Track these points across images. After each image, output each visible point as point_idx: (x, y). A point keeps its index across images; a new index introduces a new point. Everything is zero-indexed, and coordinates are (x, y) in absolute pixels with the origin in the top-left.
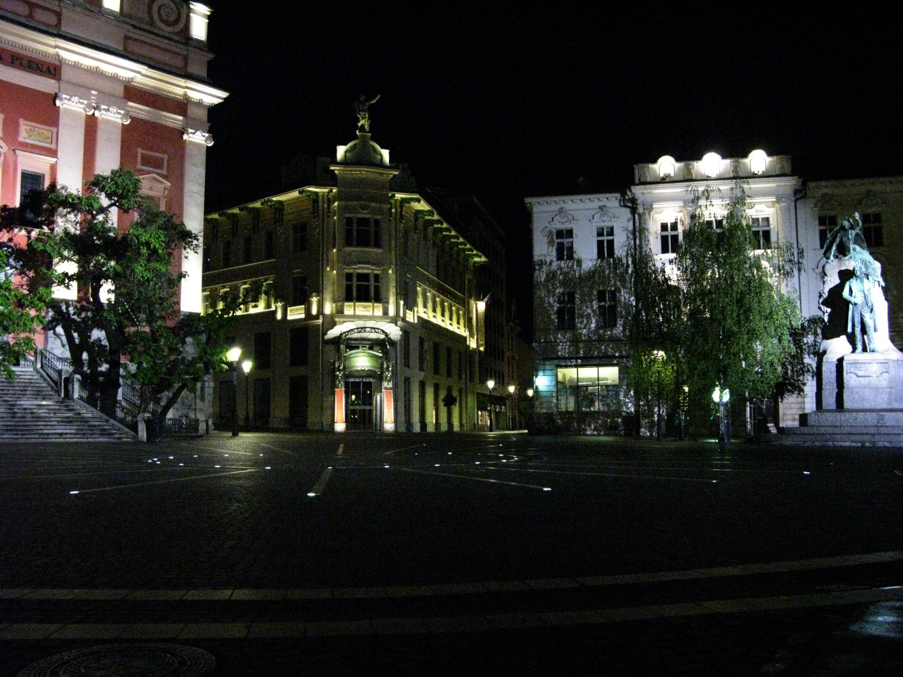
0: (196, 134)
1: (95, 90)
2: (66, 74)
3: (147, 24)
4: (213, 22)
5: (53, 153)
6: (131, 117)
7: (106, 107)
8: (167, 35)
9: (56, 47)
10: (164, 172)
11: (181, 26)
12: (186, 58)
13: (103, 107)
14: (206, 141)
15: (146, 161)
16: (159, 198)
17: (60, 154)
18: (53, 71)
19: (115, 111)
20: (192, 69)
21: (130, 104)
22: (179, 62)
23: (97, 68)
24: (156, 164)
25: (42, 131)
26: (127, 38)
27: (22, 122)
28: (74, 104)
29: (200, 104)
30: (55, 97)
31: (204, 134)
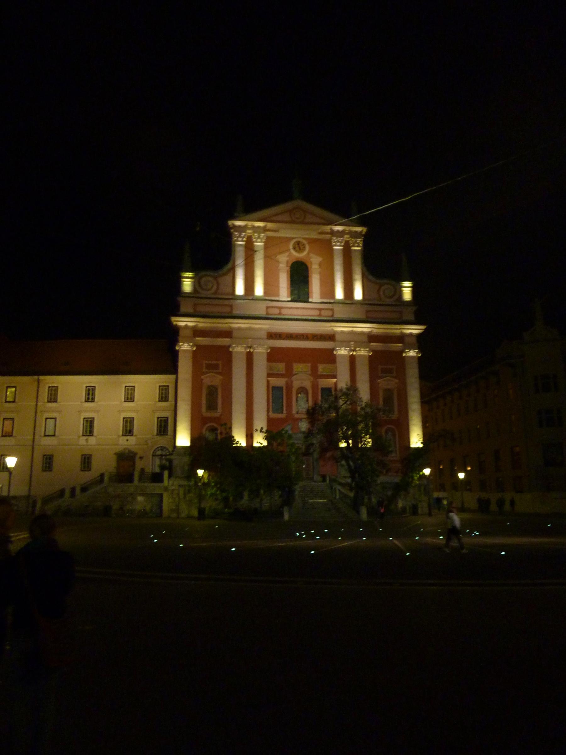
2: (338, 337)
4: (415, 291)
5: (334, 377)
6: (373, 351)
9: (331, 327)
13: (357, 349)
17: (338, 377)
20: (405, 318)
21: (372, 344)
26: (367, 312)
28: (343, 351)
29: (411, 334)
30: (333, 349)
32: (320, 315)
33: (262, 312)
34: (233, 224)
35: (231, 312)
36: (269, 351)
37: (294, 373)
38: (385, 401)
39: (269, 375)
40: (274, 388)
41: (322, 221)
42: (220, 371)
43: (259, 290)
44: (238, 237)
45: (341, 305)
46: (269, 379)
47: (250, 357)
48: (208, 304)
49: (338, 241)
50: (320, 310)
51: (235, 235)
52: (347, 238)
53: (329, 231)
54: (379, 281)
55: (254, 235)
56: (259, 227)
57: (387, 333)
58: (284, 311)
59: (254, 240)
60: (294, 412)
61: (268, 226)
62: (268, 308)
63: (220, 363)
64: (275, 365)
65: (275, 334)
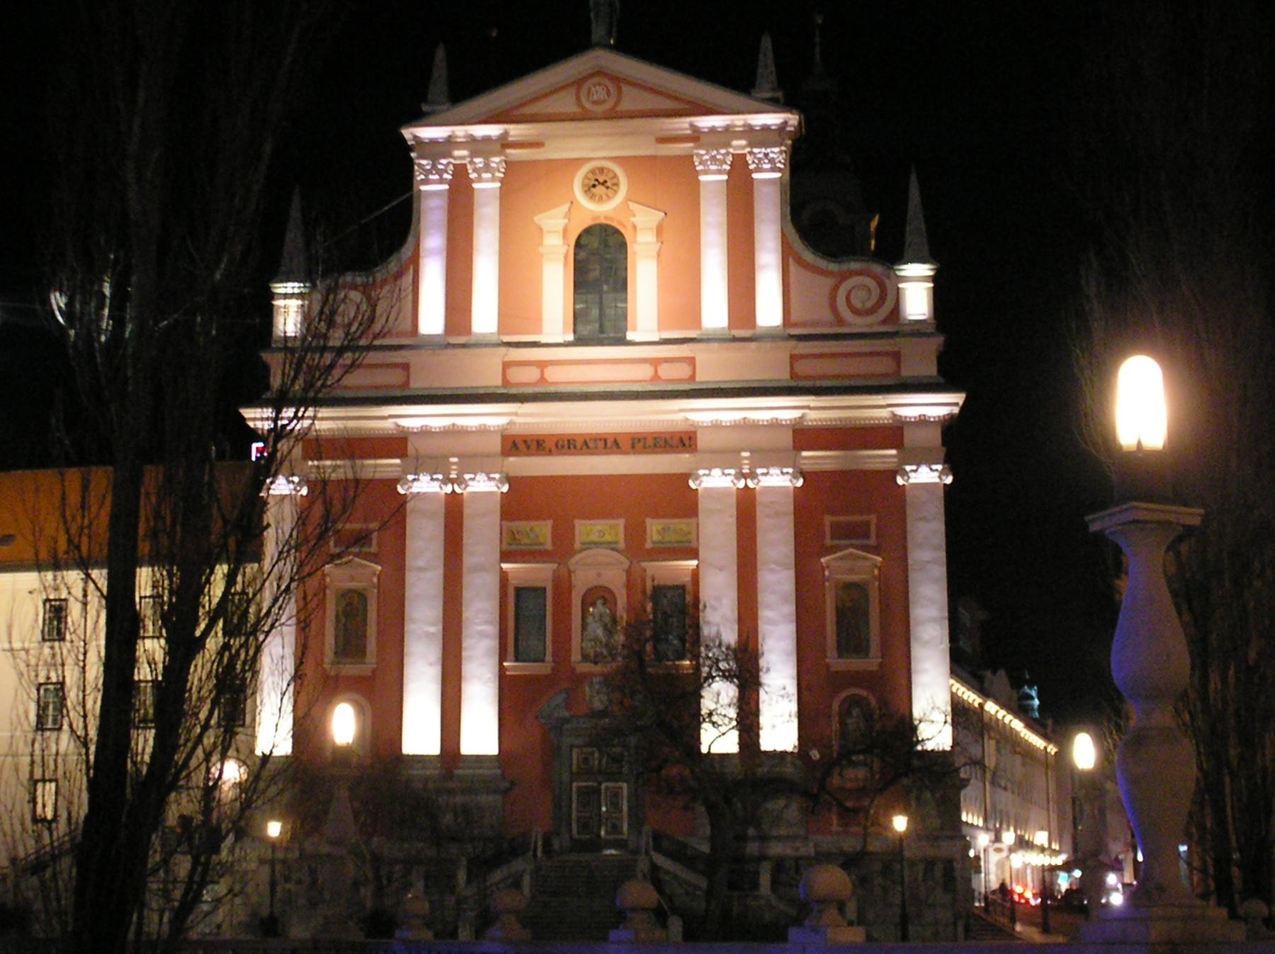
0: (920, 470)
1: (745, 451)
2: (703, 441)
3: (831, 325)
5: (694, 554)
12: (897, 356)
13: (759, 471)
14: (940, 477)
18: (687, 442)
19: (778, 471)
21: (805, 454)
23: (745, 419)
26: (794, 358)
29: (923, 422)
30: (685, 477)
31: (934, 467)
32: (656, 377)
33: (491, 379)
34: (415, 137)
35: (406, 384)
36: (505, 488)
37: (577, 546)
38: (841, 613)
40: (519, 591)
41: (669, 105)
42: (374, 549)
43: (484, 319)
44: (428, 172)
45: (715, 345)
46: (504, 566)
49: (713, 158)
50: (655, 362)
51: (420, 165)
52: (736, 148)
53: (689, 132)
54: (833, 267)
55: (471, 162)
56: (487, 139)
57: (846, 419)
58: (554, 375)
59: (473, 176)
60: (576, 656)
61: (512, 133)
62: (506, 365)
64: (523, 525)
65: (525, 442)
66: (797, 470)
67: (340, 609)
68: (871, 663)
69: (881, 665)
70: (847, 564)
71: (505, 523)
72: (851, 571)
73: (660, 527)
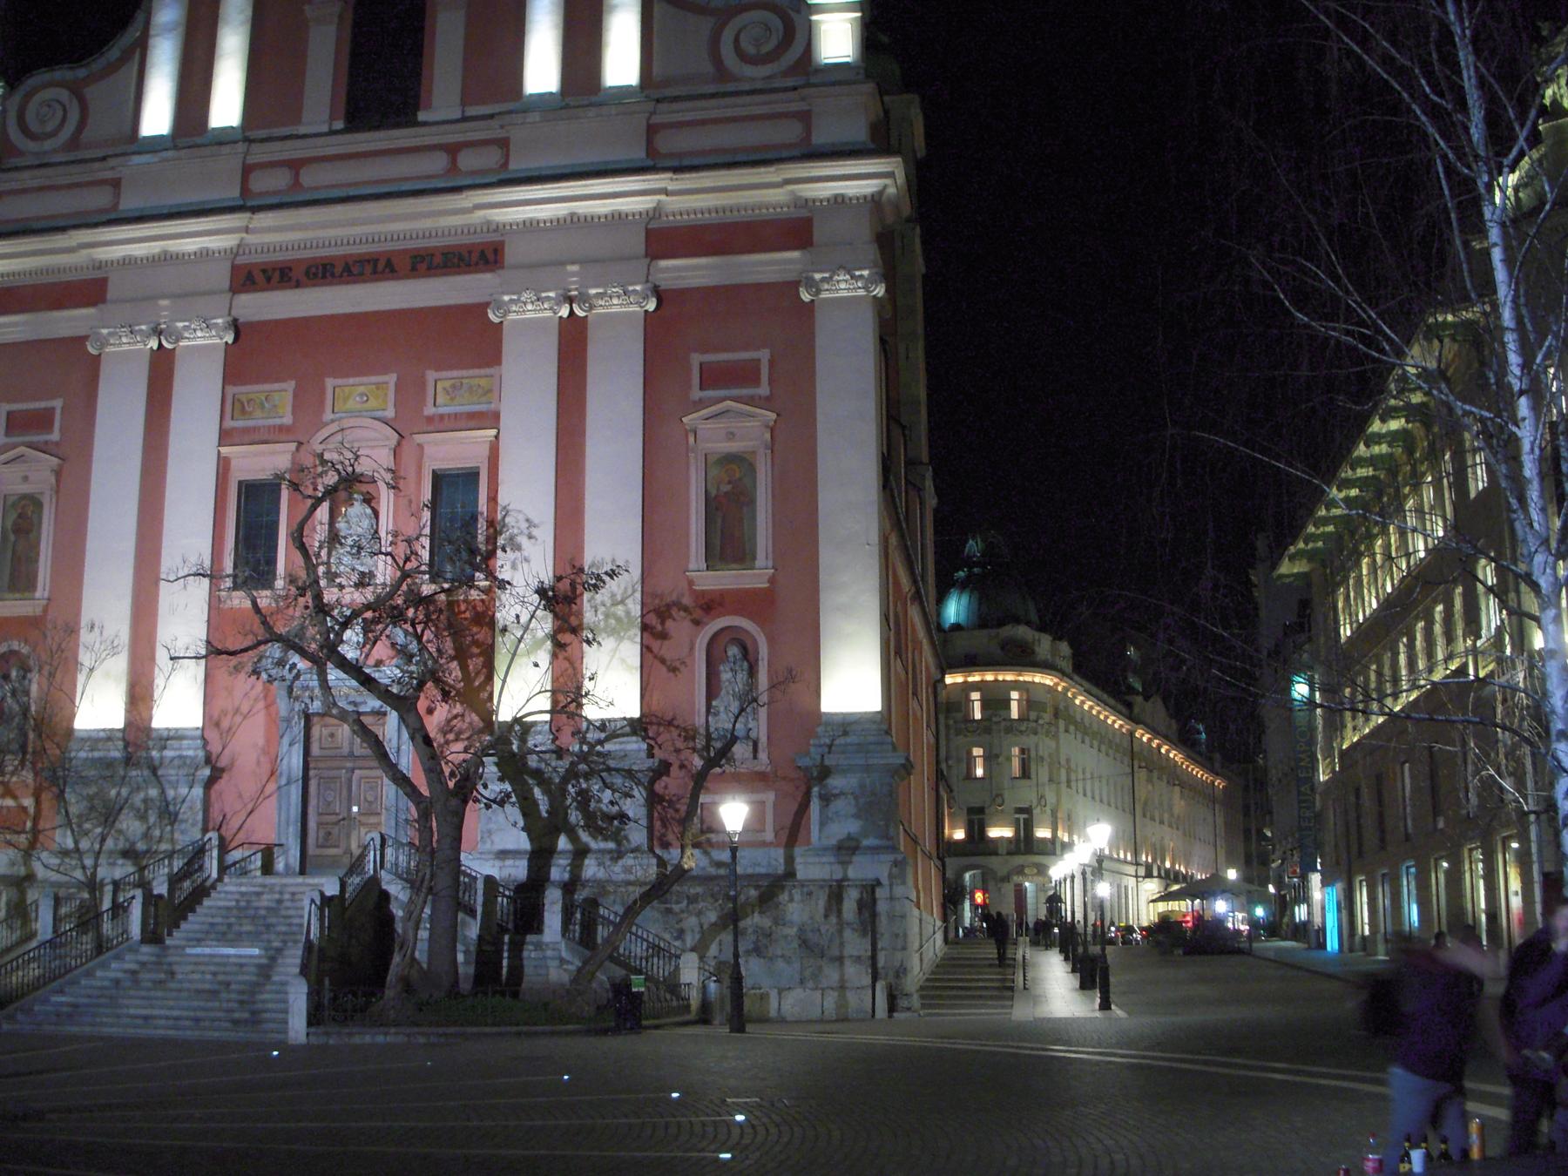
1: (573, 263)
2: (511, 254)
6: (659, 293)
7: (601, 290)
8: (759, 85)
10: (764, 390)
11: (796, 51)
12: (805, 117)
13: (593, 291)
15: (713, 377)
16: (754, 453)
18: (491, 257)
20: (822, 136)
21: (664, 263)
22: (789, 132)
24: (742, 375)
25: (476, 381)
26: (652, 130)
27: (431, 375)
29: (839, 201)
32: (453, 168)
37: (328, 416)
38: (712, 506)
39: (225, 437)
40: (247, 486)
47: (162, 369)
48: (41, 189)
50: (453, 150)
63: (58, 404)
65: (264, 271)
66: (649, 285)
67: (9, 524)
68: (753, 578)
69: (772, 580)
70: (720, 425)
71: (231, 390)
72: (731, 436)
73: (447, 384)
